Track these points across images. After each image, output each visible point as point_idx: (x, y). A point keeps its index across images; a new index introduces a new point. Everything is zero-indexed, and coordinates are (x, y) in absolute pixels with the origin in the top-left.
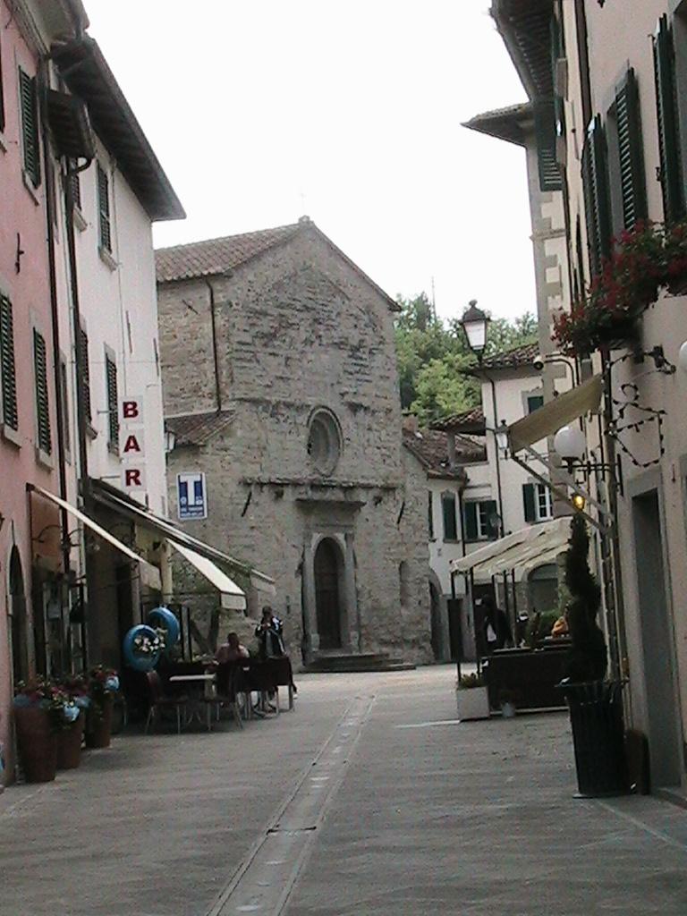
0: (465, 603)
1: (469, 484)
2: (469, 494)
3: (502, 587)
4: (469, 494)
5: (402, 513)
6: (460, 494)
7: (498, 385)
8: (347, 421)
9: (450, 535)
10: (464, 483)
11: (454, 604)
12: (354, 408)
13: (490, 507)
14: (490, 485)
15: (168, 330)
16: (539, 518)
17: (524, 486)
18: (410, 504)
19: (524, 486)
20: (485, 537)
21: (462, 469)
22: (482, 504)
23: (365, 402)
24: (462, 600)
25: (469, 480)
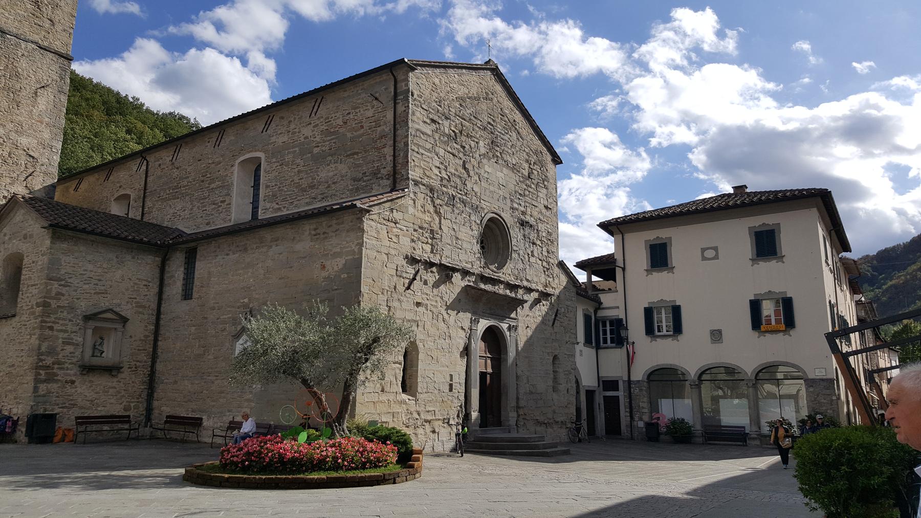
0: (597, 393)
1: (601, 307)
2: (601, 313)
3: (627, 383)
4: (601, 313)
5: (556, 315)
6: (595, 314)
7: (627, 236)
8: (516, 235)
9: (588, 341)
10: (599, 305)
11: (590, 394)
12: (523, 224)
13: (618, 326)
14: (618, 307)
15: (356, 122)
16: (657, 333)
17: (646, 309)
18: (563, 310)
19: (646, 309)
20: (614, 345)
21: (597, 294)
22: (612, 322)
23: (532, 221)
24: (595, 391)
25: (602, 303)
